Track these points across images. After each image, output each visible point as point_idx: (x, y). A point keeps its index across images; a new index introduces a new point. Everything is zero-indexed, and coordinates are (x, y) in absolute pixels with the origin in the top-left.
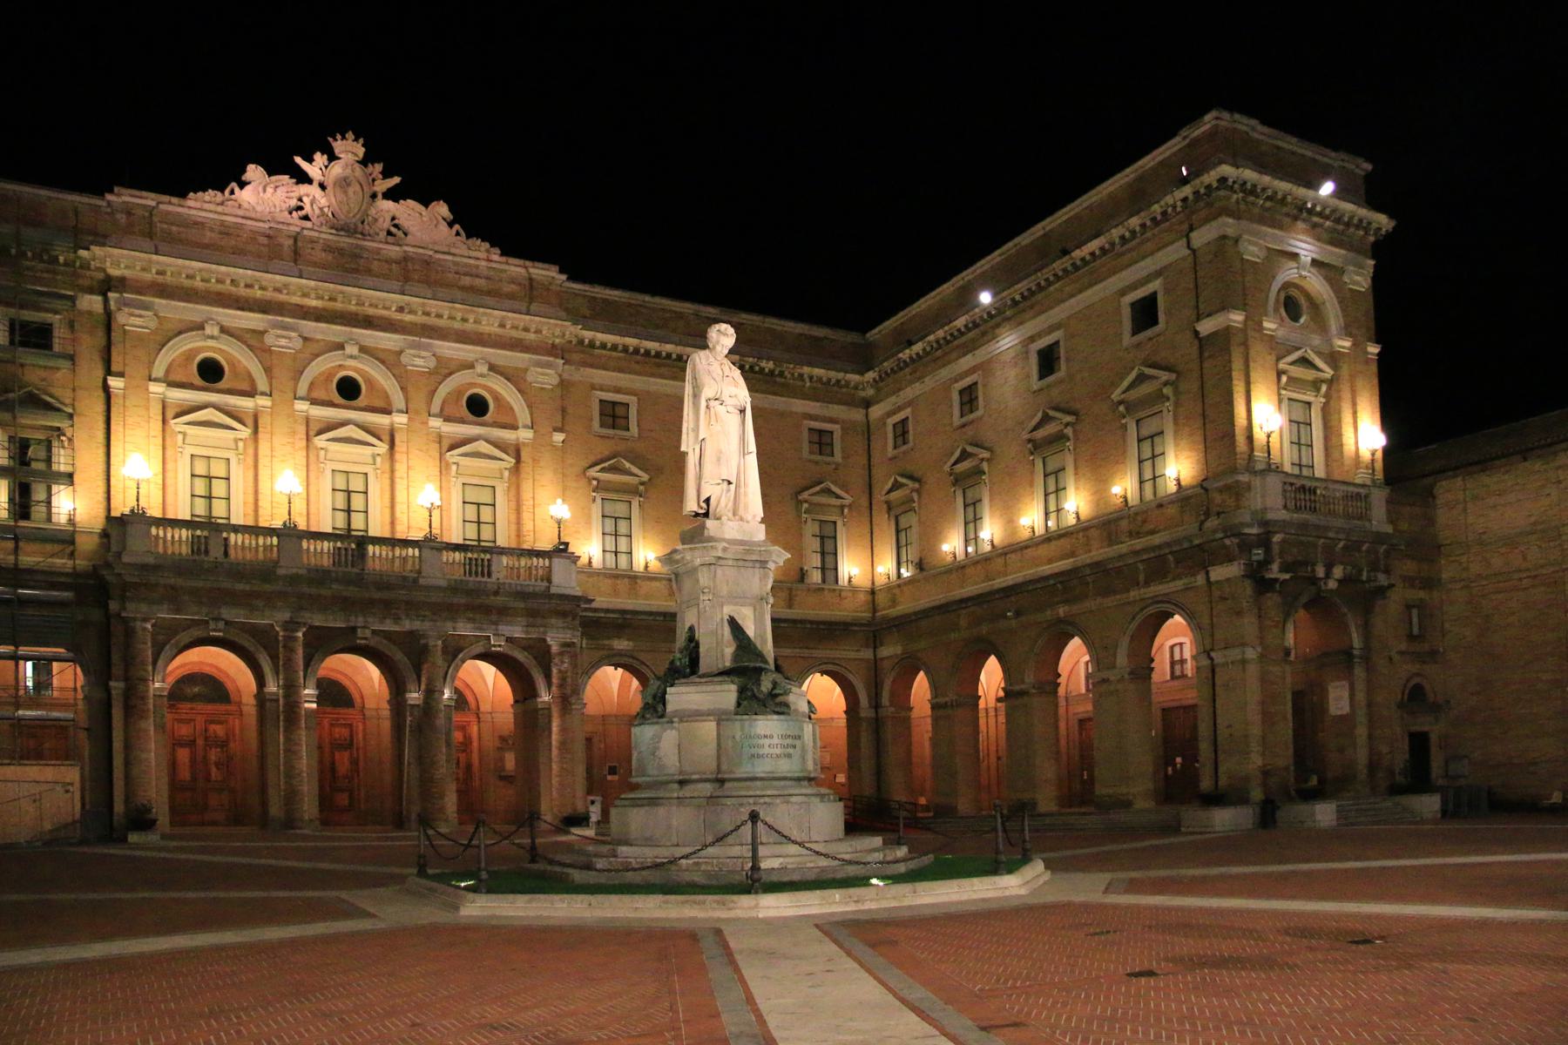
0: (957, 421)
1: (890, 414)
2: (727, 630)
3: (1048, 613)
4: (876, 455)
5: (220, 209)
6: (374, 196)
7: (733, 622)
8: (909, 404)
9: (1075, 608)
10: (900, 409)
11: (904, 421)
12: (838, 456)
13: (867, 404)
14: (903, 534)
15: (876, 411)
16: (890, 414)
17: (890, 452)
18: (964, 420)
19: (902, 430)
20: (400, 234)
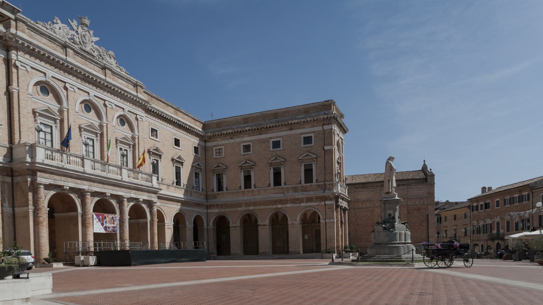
1: (216, 146)
3: (275, 206)
8: (223, 145)
9: (284, 206)
10: (219, 145)
13: (205, 142)
16: (216, 146)
19: (219, 152)
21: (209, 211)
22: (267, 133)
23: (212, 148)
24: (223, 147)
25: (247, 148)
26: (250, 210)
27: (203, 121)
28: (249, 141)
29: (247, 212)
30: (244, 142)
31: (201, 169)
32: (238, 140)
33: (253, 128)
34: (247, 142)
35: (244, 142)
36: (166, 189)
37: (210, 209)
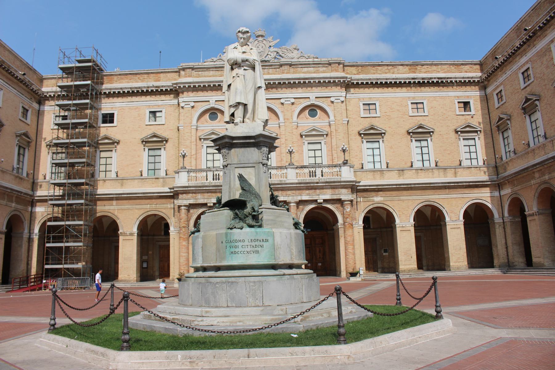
0: (523, 86)
1: (495, 89)
2: (237, 183)
4: (491, 108)
5: (215, 63)
6: (270, 46)
7: (241, 177)
8: (501, 84)
10: (498, 87)
11: (501, 91)
12: (473, 112)
14: (506, 140)
15: (489, 90)
16: (495, 90)
17: (497, 105)
18: (526, 84)
20: (279, 57)
21: (503, 193)
22: (546, 36)
23: (492, 93)
24: (501, 88)
25: (526, 75)
26: (545, 182)
27: (477, 60)
28: (527, 62)
29: (543, 187)
30: (522, 66)
31: (476, 132)
32: (515, 67)
33: (524, 40)
34: (524, 64)
35: (522, 66)
36: (397, 176)
37: (502, 189)
